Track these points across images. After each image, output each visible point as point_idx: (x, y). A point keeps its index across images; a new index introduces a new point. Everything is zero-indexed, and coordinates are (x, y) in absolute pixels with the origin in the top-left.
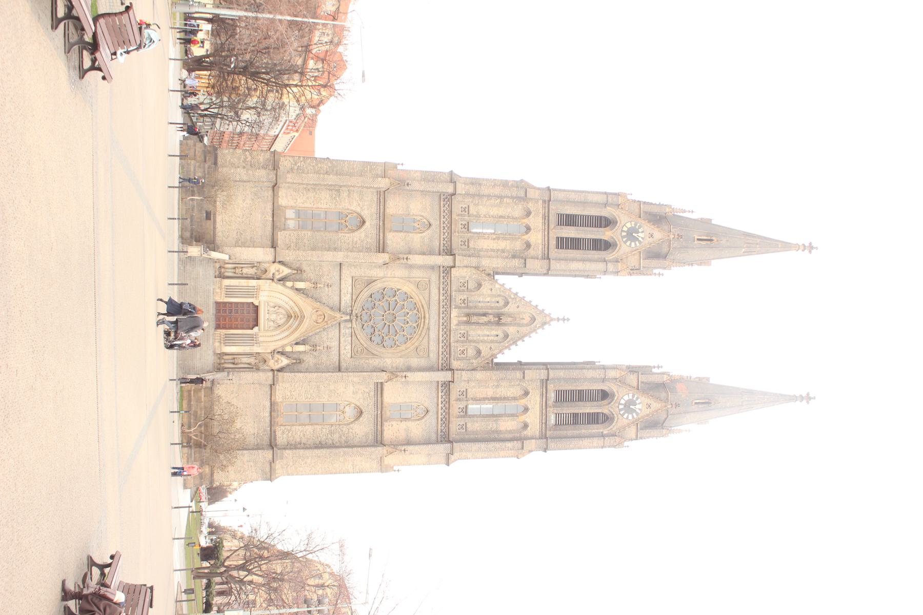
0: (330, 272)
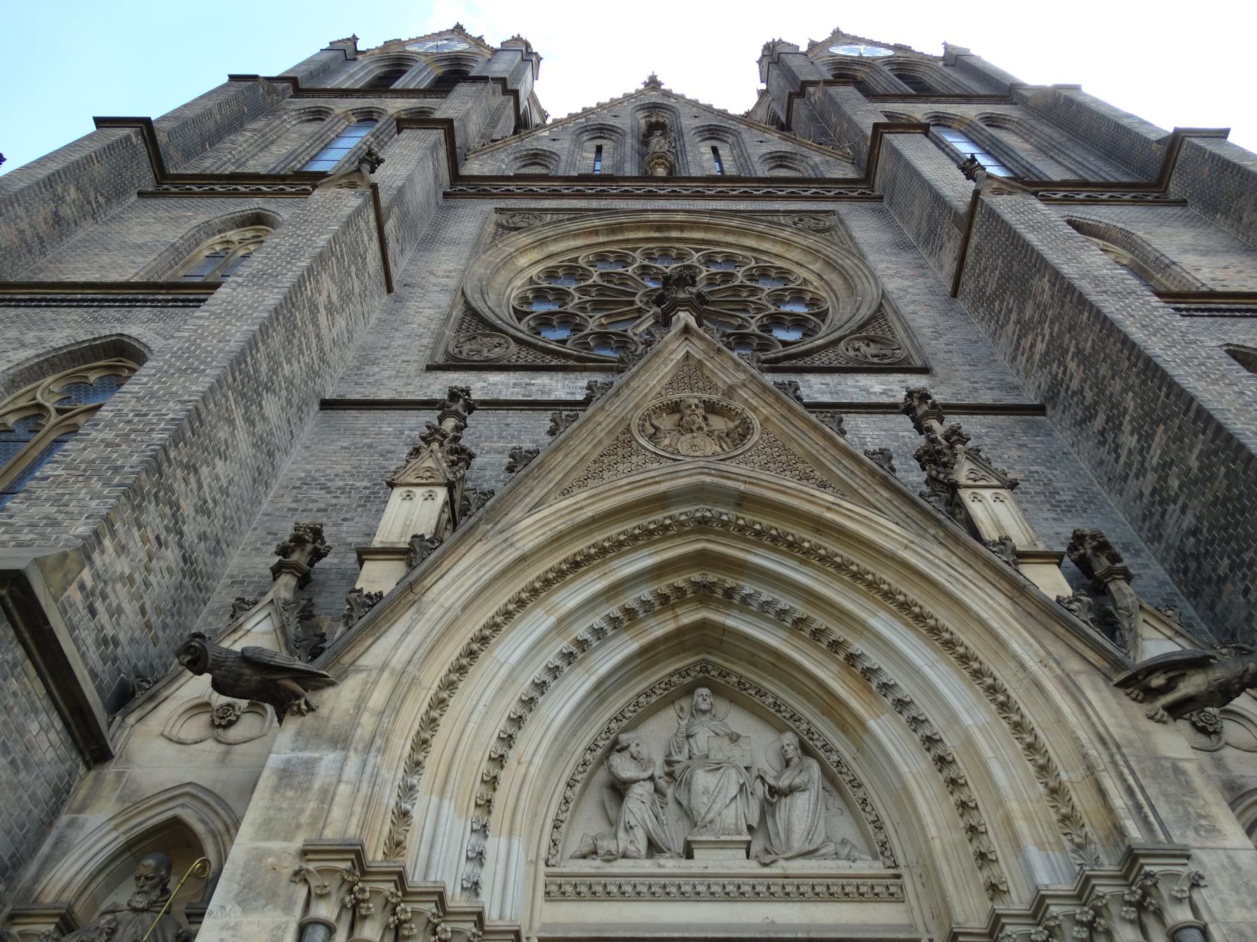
0: (370, 446)
